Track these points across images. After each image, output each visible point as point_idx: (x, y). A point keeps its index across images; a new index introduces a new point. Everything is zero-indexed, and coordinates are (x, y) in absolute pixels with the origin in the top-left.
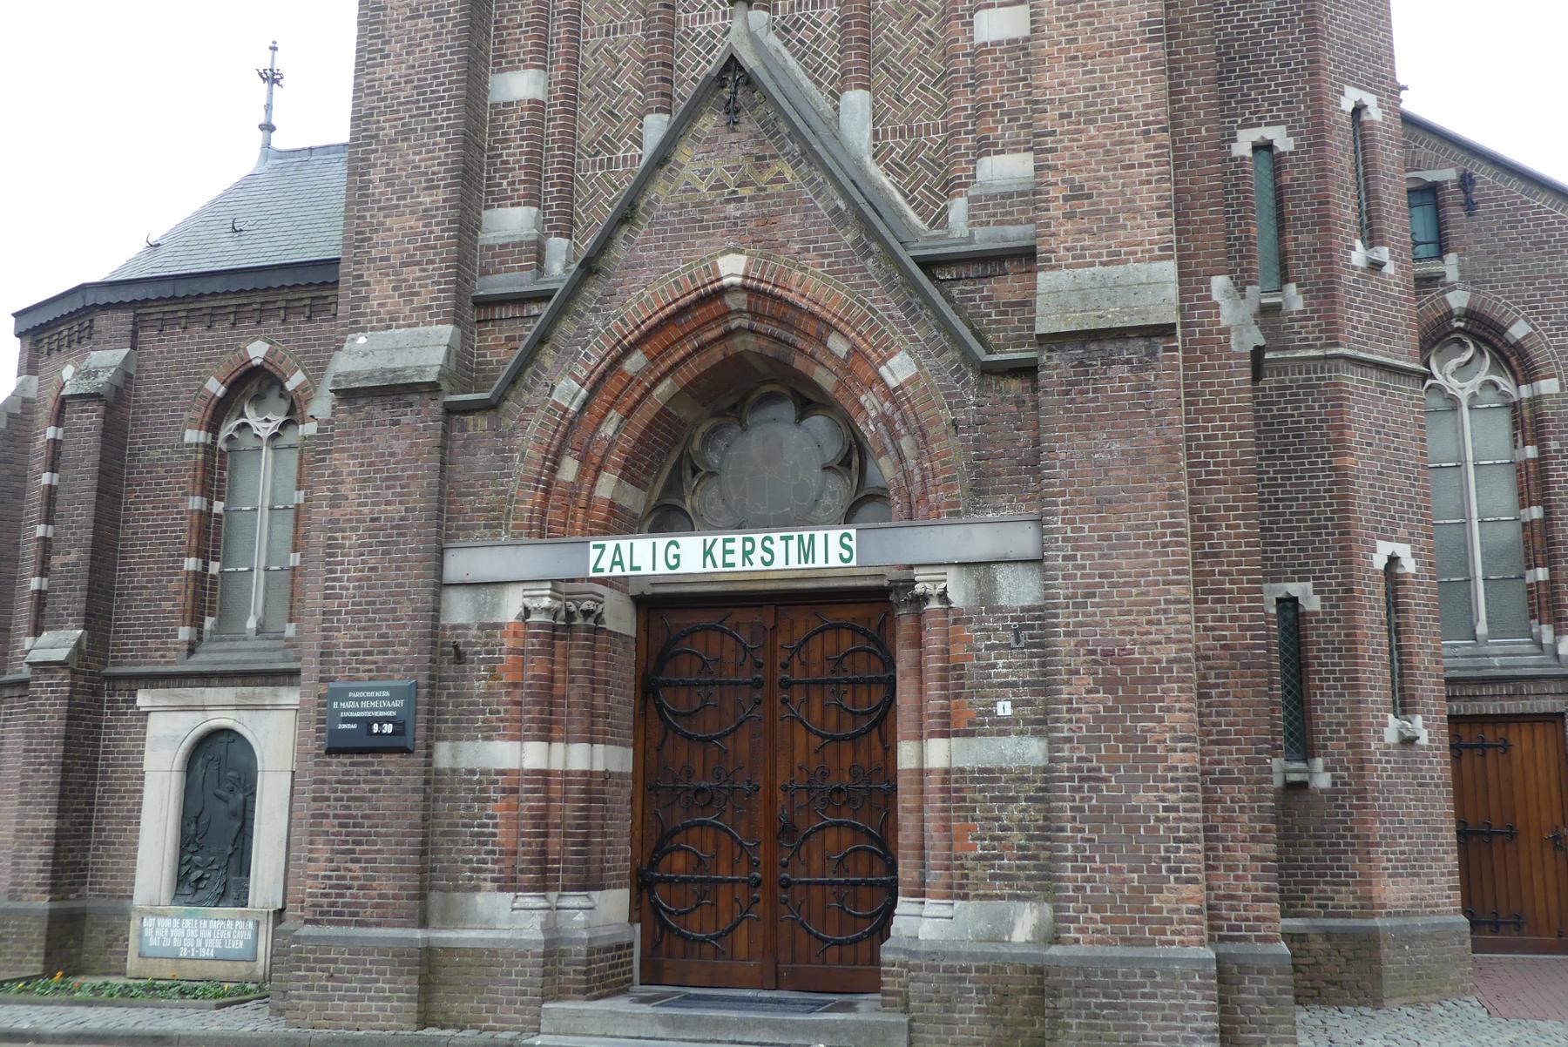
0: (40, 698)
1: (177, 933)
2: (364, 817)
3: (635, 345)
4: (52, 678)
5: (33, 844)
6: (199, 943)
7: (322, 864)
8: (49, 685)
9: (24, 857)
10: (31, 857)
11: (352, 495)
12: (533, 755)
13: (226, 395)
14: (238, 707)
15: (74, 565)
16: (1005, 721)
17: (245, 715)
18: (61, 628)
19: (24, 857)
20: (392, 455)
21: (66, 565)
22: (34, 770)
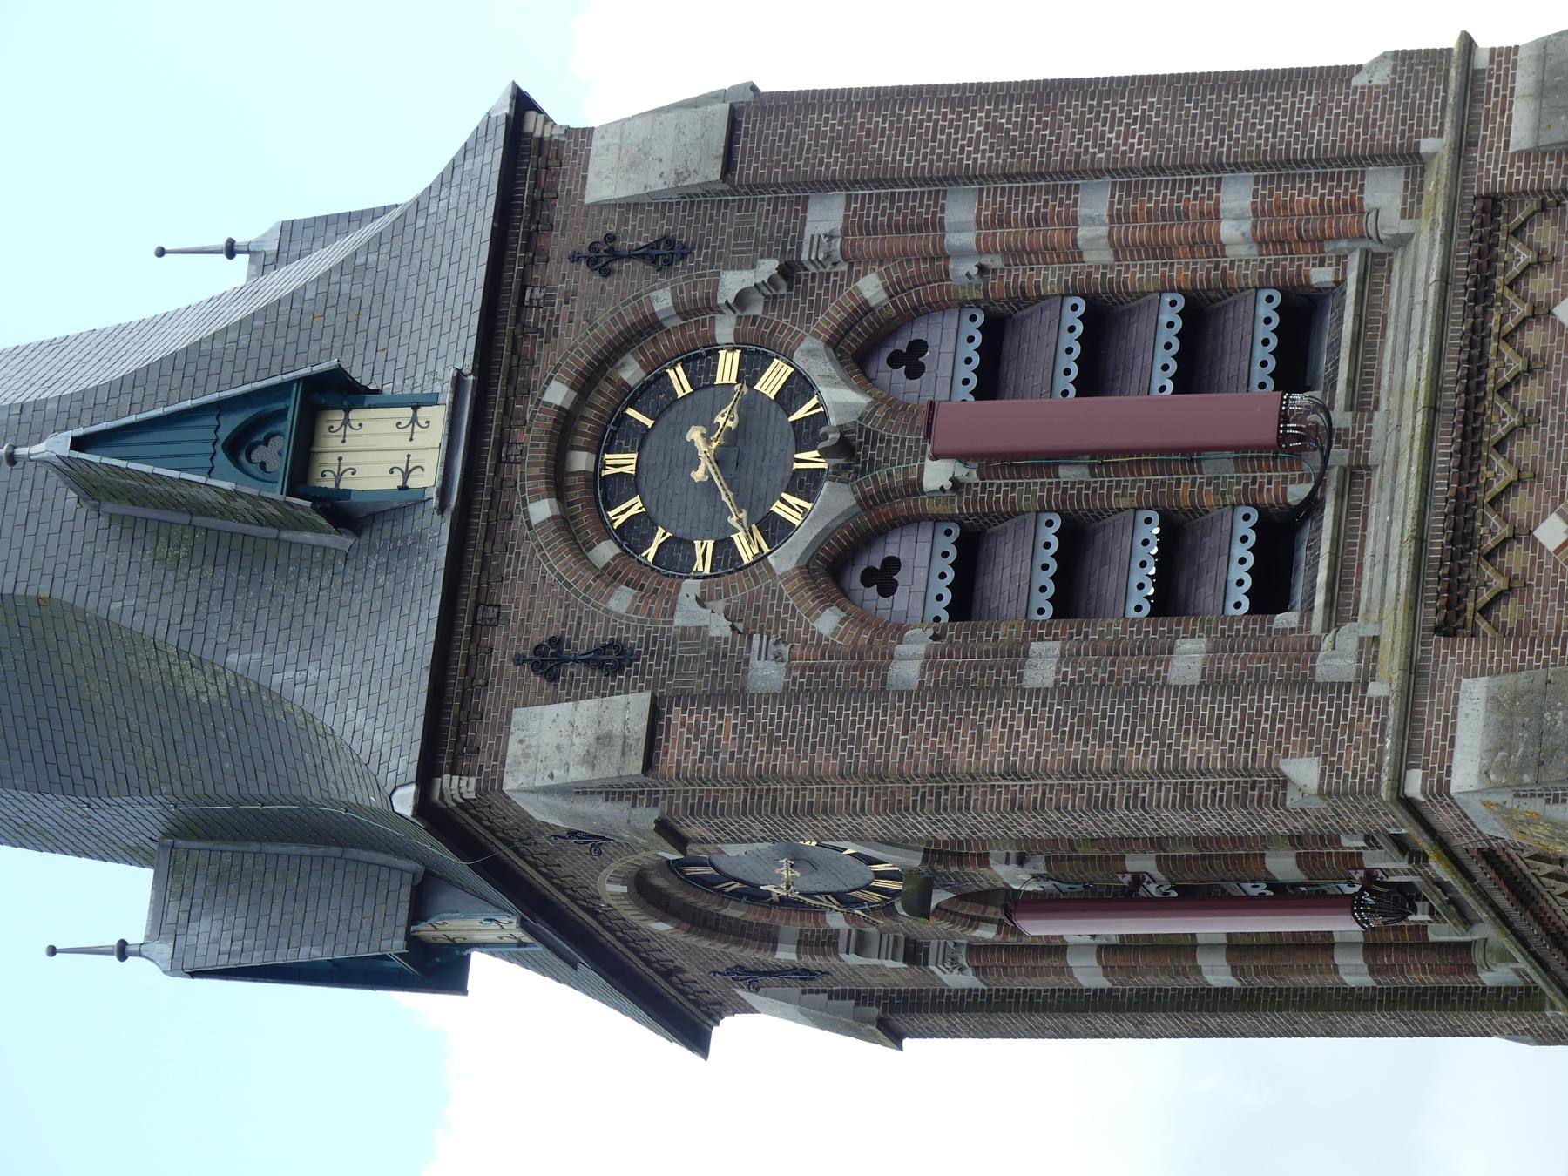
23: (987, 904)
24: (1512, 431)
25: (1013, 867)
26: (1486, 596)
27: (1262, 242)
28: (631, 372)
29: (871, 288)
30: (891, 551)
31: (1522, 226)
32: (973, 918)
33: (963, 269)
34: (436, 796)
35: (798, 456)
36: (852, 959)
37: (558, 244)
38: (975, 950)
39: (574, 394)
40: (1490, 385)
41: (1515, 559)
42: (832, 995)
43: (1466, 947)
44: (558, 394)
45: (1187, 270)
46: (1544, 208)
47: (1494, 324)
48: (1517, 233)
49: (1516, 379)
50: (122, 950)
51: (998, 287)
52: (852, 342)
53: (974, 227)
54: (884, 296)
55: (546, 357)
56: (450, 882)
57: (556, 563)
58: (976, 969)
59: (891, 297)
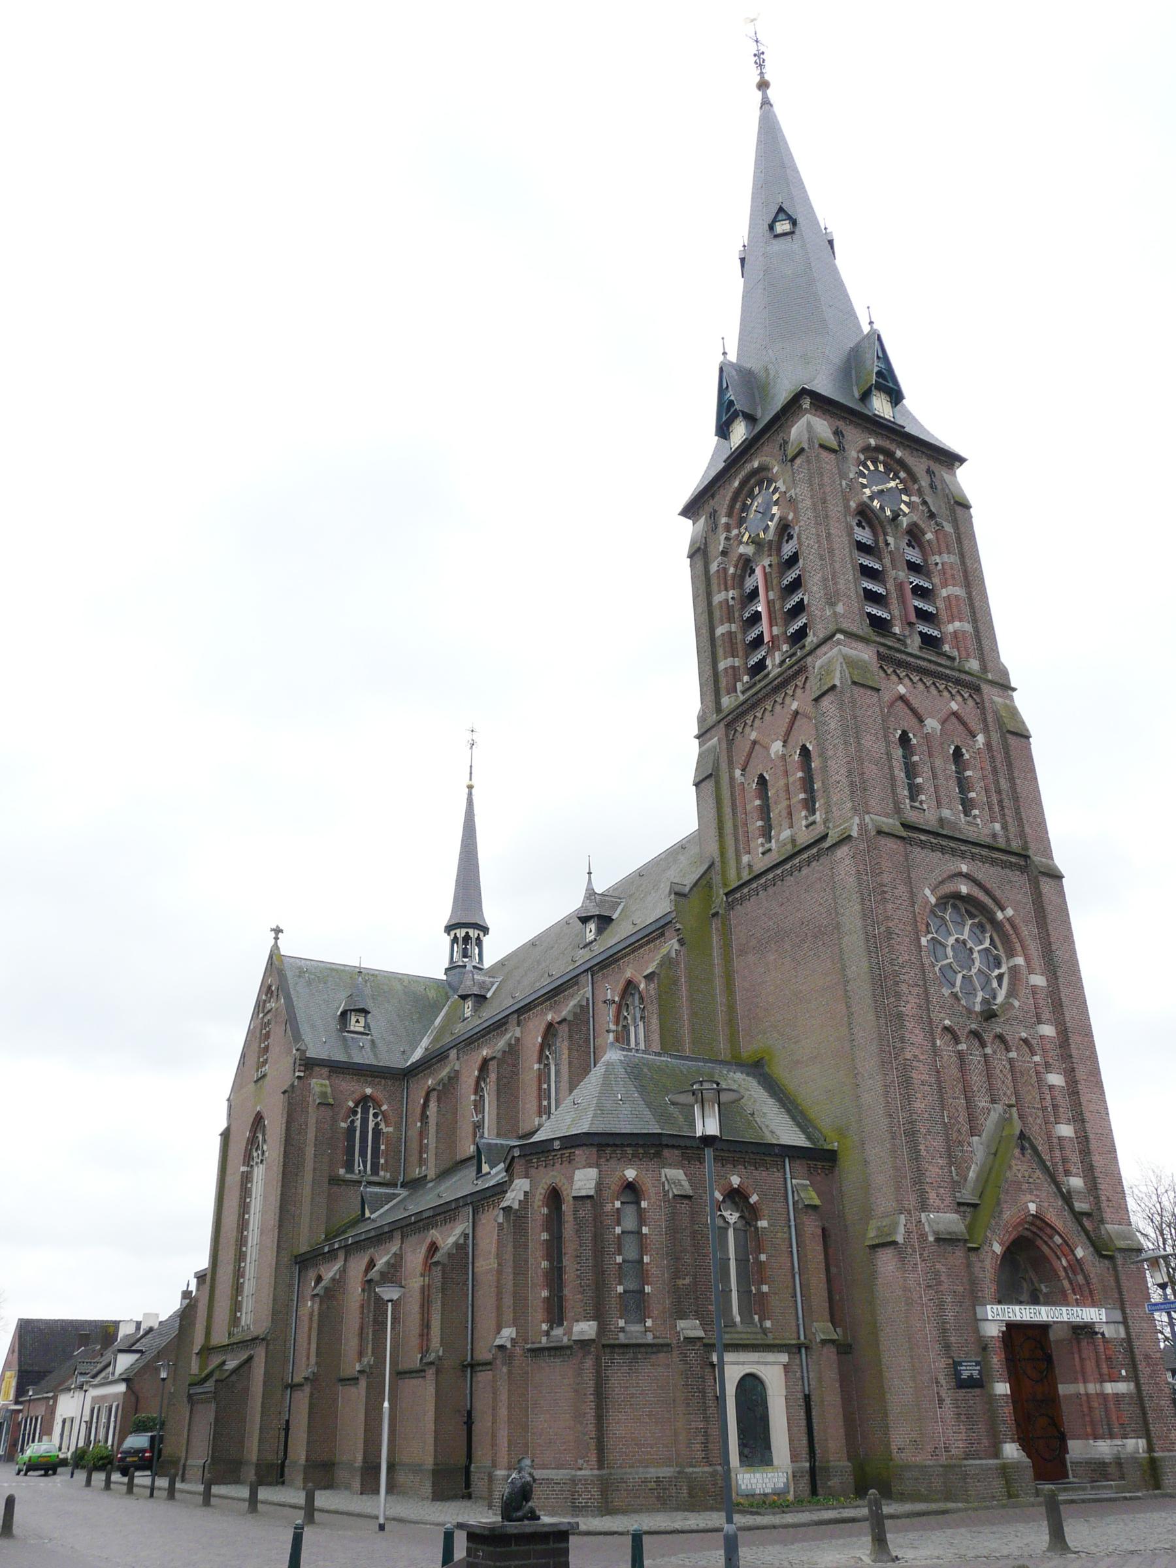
0: (689, 1357)
1: (754, 1481)
2: (974, 1414)
3: (1065, 1241)
4: (694, 1346)
5: (697, 1436)
6: (764, 1485)
7: (964, 1434)
8: (692, 1350)
9: (694, 1443)
10: (697, 1443)
11: (945, 1281)
12: (1109, 1388)
13: (749, 1203)
14: (758, 1363)
15: (689, 1285)
16: (1123, 1377)
17: (762, 1367)
18: (687, 1319)
19: (694, 1443)
20: (955, 1266)
21: (683, 1285)
22: (692, 1396)
23: (742, 570)
24: (925, 684)
25: (769, 563)
26: (885, 668)
27: (955, 632)
28: (902, 475)
29: (929, 536)
30: (867, 528)
31: (972, 697)
33: (937, 559)
34: (805, 396)
36: (724, 535)
37: (931, 463)
38: (725, 570)
39: (898, 457)
41: (894, 677)
43: (736, 692)
44: (899, 454)
45: (944, 615)
46: (977, 703)
48: (970, 696)
49: (937, 687)
50: (724, 354)
51: (932, 567)
52: (915, 530)
55: (907, 453)
56: (754, 426)
57: (861, 444)
59: (927, 541)
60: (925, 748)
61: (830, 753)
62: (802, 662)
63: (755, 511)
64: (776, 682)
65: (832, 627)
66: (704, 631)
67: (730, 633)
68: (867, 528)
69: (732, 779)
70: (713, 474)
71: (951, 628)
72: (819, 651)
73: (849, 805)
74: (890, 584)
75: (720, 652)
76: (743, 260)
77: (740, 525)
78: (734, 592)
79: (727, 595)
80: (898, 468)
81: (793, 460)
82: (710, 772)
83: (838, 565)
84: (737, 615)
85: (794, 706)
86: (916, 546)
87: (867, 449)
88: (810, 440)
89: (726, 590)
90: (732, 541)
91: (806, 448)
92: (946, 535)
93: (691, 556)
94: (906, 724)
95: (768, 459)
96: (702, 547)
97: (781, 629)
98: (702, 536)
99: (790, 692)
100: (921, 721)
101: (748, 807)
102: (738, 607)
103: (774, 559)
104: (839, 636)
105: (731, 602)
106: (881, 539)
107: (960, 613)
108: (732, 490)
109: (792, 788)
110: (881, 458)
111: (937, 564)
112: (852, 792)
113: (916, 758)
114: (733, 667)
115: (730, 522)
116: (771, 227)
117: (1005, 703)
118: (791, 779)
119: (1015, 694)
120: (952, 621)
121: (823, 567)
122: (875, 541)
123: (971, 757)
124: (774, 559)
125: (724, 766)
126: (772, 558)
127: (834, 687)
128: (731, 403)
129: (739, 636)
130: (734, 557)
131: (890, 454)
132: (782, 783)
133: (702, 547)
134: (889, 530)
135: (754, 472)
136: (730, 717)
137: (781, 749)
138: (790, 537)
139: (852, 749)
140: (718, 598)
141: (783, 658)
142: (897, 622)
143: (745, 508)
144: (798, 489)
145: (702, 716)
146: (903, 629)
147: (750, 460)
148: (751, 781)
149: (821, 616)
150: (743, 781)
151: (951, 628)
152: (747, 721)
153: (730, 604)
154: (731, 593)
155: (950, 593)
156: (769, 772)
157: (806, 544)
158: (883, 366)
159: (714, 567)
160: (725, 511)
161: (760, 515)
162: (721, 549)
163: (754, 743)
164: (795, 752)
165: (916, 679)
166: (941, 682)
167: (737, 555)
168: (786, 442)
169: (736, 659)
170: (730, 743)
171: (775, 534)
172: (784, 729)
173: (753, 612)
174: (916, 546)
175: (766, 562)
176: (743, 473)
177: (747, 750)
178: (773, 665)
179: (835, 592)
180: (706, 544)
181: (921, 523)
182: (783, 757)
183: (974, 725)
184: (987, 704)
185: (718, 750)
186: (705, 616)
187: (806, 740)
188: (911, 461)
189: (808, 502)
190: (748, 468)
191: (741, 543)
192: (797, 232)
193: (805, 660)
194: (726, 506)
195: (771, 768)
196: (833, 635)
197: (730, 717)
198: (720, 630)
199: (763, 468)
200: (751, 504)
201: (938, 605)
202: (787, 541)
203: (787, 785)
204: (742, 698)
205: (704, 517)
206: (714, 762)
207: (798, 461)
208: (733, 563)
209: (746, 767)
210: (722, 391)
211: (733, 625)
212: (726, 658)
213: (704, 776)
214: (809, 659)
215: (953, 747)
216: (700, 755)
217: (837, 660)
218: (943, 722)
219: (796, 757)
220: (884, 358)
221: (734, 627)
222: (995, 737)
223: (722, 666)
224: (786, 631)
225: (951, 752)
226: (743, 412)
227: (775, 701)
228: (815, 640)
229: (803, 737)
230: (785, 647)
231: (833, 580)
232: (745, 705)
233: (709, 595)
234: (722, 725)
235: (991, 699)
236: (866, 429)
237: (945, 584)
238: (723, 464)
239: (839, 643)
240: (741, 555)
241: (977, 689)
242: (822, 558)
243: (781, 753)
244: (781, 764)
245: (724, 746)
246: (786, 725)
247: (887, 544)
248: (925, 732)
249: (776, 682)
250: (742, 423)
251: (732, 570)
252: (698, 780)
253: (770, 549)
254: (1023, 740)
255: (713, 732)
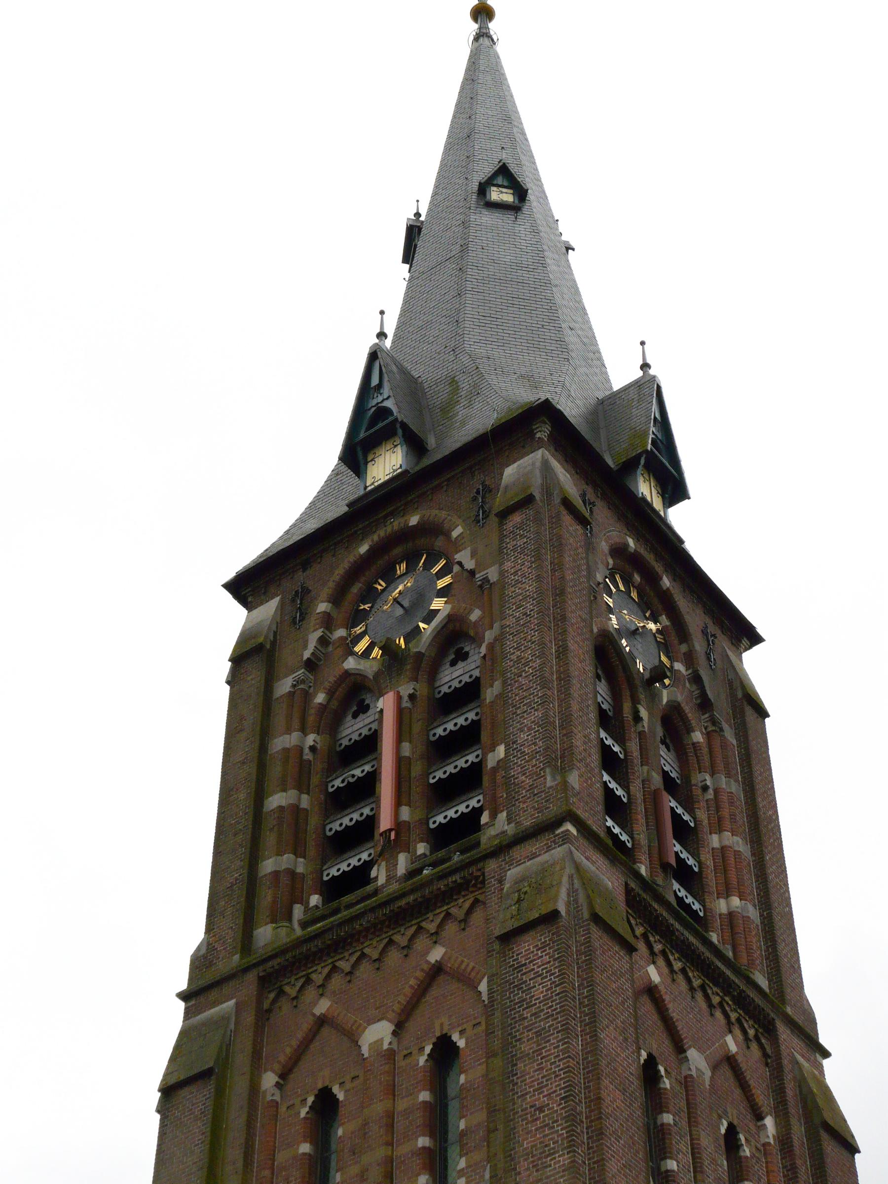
25: (412, 691)
29: (698, 736)
30: (603, 680)
32: (334, 693)
35: (641, 664)
36: (319, 633)
38: (307, 696)
39: (665, 588)
40: (707, 982)
42: (275, 633)
45: (711, 880)
47: (727, 999)
53: (729, 790)
54: (695, 741)
58: (294, 692)
59: (693, 744)
60: (683, 1104)
61: (525, 1047)
62: (473, 869)
63: (395, 600)
64: (402, 903)
65: (554, 809)
66: (242, 796)
67: (296, 809)
68: (603, 680)
69: (254, 1089)
70: (312, 526)
71: (722, 906)
72: (518, 852)
73: (564, 1159)
74: (636, 788)
75: (270, 839)
76: (413, 232)
77: (358, 617)
78: (318, 739)
79: (303, 742)
80: (660, 607)
81: (504, 514)
82: (211, 1064)
83: (575, 707)
84: (315, 780)
85: (436, 954)
86: (671, 747)
87: (619, 551)
88: (547, 491)
89: (304, 730)
90: (330, 648)
91: (538, 496)
92: (724, 745)
93: (239, 659)
94: (655, 1046)
95: (443, 514)
96: (268, 646)
97: (419, 814)
98: (269, 628)
99: (431, 927)
100: (680, 1049)
101: (281, 1157)
102: (319, 766)
103: (422, 689)
104: (569, 827)
105: (308, 755)
106: (627, 707)
107: (740, 882)
108: (352, 558)
109: (400, 1124)
110: (637, 578)
111: (705, 788)
112: (571, 1132)
113: (667, 1118)
114: (291, 873)
115: (334, 615)
116: (482, 190)
117: (813, 1072)
118: (402, 1105)
119: (826, 1063)
120: (727, 893)
121: (545, 701)
122: (614, 708)
123: (753, 1156)
124: (422, 689)
125: (241, 1059)
126: (418, 686)
127: (552, 916)
128: (383, 412)
129: (314, 821)
130: (330, 676)
131: (652, 579)
132: (379, 1108)
133: (268, 646)
134: (642, 696)
135: (406, 535)
136: (275, 963)
137: (388, 1039)
138: (462, 656)
139: (578, 1045)
140: (282, 742)
141: (416, 865)
142: (643, 857)
143: (370, 595)
144: (508, 565)
145: (204, 957)
146: (651, 869)
147: (405, 511)
148: (297, 1101)
149: (532, 787)
150: (277, 1098)
151: (722, 906)
152: (314, 976)
153: (305, 757)
154: (311, 739)
155: (726, 843)
156: (348, 1085)
157: (514, 657)
158: (659, 436)
159: (284, 686)
160: (330, 591)
161: (399, 611)
162: (307, 654)
163: (322, 1021)
164: (422, 1049)
165: (678, 965)
166: (715, 989)
167: (337, 673)
168: (488, 491)
169: (302, 860)
170: (263, 1016)
171: (430, 644)
172: (402, 999)
173: (351, 780)
174: (671, 747)
175: (406, 690)
176: (381, 533)
177: (300, 1035)
178: (389, 878)
179: (563, 750)
180: (274, 643)
181: (687, 709)
182: (390, 1055)
183: (763, 1097)
184: (785, 1062)
185: (232, 1027)
186: (251, 769)
187: (452, 1027)
188: (683, 603)
189: (530, 587)
190: (395, 525)
191: (353, 653)
192: (525, 209)
193: (480, 865)
194: (331, 584)
195: (354, 1078)
196: (559, 823)
197: (275, 963)
198: (276, 800)
199: (431, 529)
200: (383, 591)
201: (703, 859)
202: (453, 663)
203: (390, 1115)
204: (299, 932)
205: (278, 599)
206: (221, 1048)
207: (516, 518)
208: (327, 685)
209: (290, 1071)
210: (366, 390)
211: (305, 797)
212: (280, 853)
213: (195, 1071)
214: (491, 866)
215: (725, 1124)
216: (184, 1034)
217: (563, 869)
218: (715, 1068)
219: (422, 1060)
220: (664, 423)
221: (305, 801)
222: (798, 1131)
223: (268, 866)
224: (428, 820)
225: (723, 1131)
226: (404, 425)
227: (391, 942)
228: (510, 829)
229: (444, 1020)
230: (421, 848)
231: (562, 727)
232: (319, 943)
233: (265, 735)
234: (252, 977)
235: (793, 1057)
236: (621, 517)
237: (718, 827)
238: (346, 509)
239: (566, 838)
240: (347, 674)
241: (768, 1029)
242: (545, 684)
243: (386, 1046)
244: (387, 1068)
245: (249, 1018)
246: (408, 991)
247: (637, 718)
248: (685, 1072)
249: (402, 903)
250: (399, 450)
251: (320, 698)
252: (173, 1080)
253: (417, 668)
254: (845, 1153)
255: (226, 989)
